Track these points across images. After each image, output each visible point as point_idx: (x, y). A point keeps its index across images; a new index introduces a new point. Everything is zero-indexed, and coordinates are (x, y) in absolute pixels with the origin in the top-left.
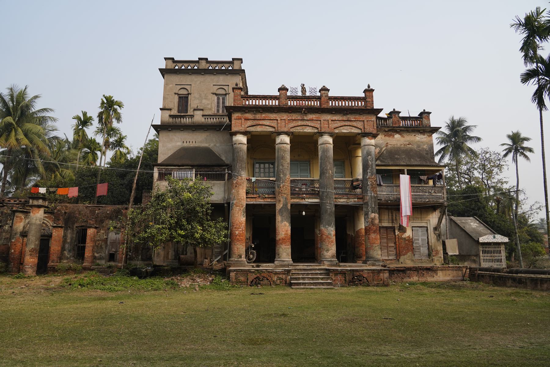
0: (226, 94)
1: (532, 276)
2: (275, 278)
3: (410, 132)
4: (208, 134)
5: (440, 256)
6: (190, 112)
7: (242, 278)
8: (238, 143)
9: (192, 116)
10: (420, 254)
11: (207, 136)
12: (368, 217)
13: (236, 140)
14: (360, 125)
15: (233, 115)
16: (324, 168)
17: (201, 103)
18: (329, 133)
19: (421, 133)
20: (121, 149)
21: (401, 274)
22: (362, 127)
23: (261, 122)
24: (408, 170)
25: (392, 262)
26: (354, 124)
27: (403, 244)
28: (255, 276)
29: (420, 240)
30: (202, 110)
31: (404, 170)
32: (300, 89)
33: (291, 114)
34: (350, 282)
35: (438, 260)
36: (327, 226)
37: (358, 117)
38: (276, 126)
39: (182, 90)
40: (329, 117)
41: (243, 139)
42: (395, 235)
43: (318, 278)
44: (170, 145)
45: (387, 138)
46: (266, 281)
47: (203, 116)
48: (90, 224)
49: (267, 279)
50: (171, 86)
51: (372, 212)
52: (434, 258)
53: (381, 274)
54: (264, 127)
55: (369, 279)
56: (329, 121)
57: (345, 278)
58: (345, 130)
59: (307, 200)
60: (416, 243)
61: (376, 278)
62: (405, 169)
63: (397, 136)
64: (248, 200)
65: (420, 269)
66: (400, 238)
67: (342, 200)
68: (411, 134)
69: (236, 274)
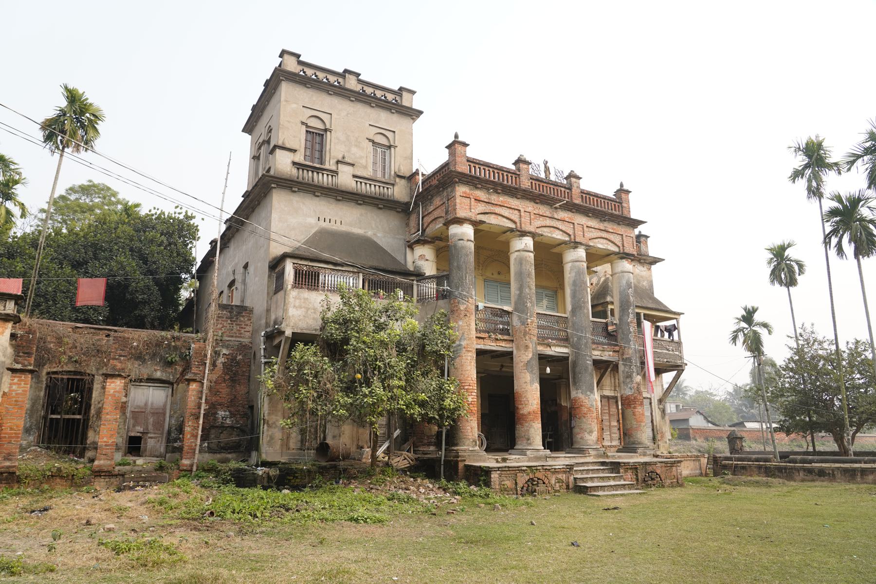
0: (390, 147)
1: (842, 465)
4: (363, 211)
6: (330, 165)
7: (508, 483)
8: (465, 239)
9: (335, 173)
11: (361, 215)
12: (632, 381)
13: (455, 235)
14: (617, 239)
15: (457, 188)
16: (579, 300)
17: (349, 151)
19: (640, 263)
20: (9, 205)
22: (620, 244)
23: (498, 210)
24: (645, 315)
30: (353, 165)
32: (542, 168)
33: (539, 206)
34: (644, 481)
36: (588, 393)
38: (517, 220)
39: (313, 119)
41: (468, 231)
44: (293, 221)
46: (541, 488)
47: (354, 176)
48: (114, 368)
50: (294, 106)
53: (674, 469)
54: (500, 218)
57: (637, 475)
59: (553, 348)
69: (500, 475)
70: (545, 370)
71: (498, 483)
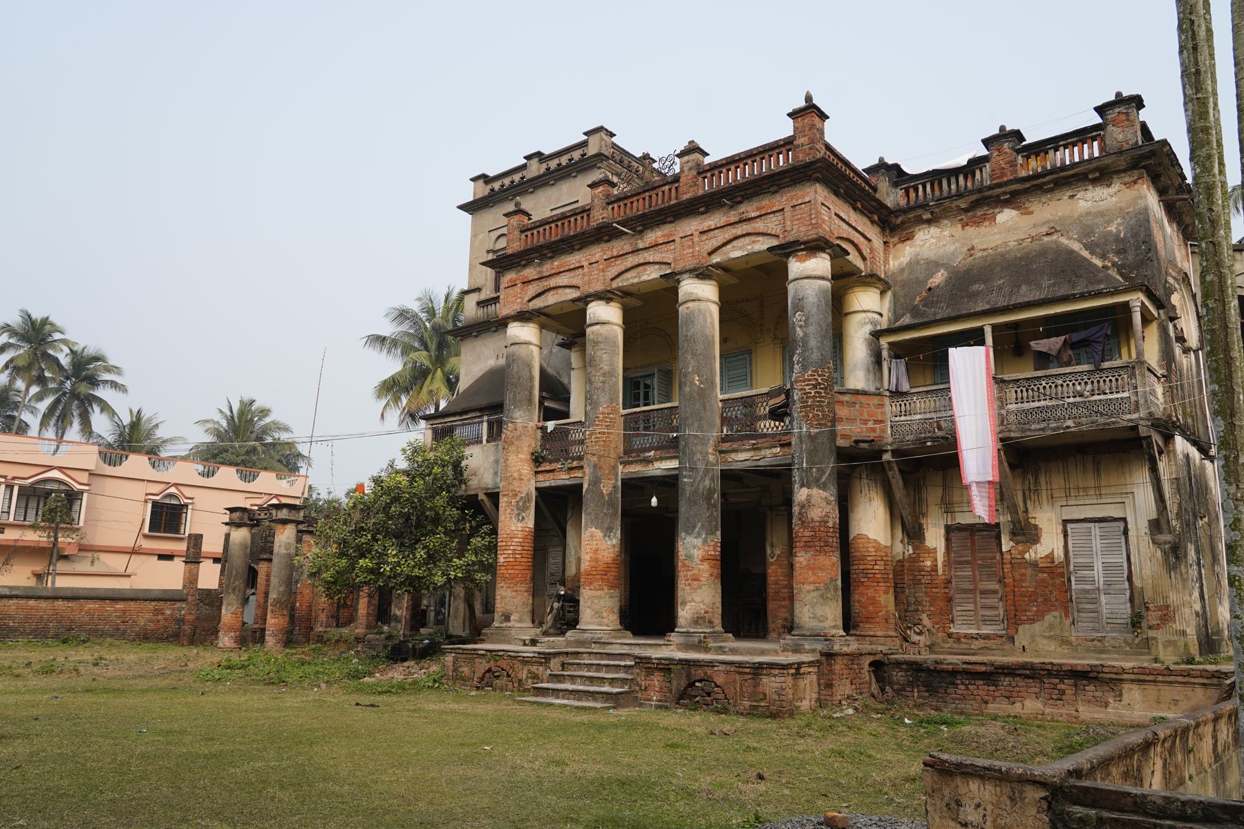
3: (1051, 190)
5: (1178, 626)
10: (1096, 620)
18: (690, 271)
19: (1095, 182)
23: (552, 282)
24: (995, 328)
25: (990, 643)
26: (759, 226)
27: (1028, 585)
28: (487, 666)
29: (1098, 566)
31: (980, 331)
35: (1169, 643)
37: (767, 203)
40: (692, 225)
42: (1002, 553)
43: (602, 680)
45: (970, 230)
49: (508, 676)
51: (802, 486)
52: (1151, 633)
54: (560, 291)
55: (731, 692)
56: (693, 239)
58: (735, 252)
59: (657, 465)
60: (1080, 580)
61: (750, 689)
62: (987, 324)
63: (1006, 216)
64: (540, 477)
65: (1050, 674)
67: (742, 456)
68: (1058, 194)
71: (451, 668)
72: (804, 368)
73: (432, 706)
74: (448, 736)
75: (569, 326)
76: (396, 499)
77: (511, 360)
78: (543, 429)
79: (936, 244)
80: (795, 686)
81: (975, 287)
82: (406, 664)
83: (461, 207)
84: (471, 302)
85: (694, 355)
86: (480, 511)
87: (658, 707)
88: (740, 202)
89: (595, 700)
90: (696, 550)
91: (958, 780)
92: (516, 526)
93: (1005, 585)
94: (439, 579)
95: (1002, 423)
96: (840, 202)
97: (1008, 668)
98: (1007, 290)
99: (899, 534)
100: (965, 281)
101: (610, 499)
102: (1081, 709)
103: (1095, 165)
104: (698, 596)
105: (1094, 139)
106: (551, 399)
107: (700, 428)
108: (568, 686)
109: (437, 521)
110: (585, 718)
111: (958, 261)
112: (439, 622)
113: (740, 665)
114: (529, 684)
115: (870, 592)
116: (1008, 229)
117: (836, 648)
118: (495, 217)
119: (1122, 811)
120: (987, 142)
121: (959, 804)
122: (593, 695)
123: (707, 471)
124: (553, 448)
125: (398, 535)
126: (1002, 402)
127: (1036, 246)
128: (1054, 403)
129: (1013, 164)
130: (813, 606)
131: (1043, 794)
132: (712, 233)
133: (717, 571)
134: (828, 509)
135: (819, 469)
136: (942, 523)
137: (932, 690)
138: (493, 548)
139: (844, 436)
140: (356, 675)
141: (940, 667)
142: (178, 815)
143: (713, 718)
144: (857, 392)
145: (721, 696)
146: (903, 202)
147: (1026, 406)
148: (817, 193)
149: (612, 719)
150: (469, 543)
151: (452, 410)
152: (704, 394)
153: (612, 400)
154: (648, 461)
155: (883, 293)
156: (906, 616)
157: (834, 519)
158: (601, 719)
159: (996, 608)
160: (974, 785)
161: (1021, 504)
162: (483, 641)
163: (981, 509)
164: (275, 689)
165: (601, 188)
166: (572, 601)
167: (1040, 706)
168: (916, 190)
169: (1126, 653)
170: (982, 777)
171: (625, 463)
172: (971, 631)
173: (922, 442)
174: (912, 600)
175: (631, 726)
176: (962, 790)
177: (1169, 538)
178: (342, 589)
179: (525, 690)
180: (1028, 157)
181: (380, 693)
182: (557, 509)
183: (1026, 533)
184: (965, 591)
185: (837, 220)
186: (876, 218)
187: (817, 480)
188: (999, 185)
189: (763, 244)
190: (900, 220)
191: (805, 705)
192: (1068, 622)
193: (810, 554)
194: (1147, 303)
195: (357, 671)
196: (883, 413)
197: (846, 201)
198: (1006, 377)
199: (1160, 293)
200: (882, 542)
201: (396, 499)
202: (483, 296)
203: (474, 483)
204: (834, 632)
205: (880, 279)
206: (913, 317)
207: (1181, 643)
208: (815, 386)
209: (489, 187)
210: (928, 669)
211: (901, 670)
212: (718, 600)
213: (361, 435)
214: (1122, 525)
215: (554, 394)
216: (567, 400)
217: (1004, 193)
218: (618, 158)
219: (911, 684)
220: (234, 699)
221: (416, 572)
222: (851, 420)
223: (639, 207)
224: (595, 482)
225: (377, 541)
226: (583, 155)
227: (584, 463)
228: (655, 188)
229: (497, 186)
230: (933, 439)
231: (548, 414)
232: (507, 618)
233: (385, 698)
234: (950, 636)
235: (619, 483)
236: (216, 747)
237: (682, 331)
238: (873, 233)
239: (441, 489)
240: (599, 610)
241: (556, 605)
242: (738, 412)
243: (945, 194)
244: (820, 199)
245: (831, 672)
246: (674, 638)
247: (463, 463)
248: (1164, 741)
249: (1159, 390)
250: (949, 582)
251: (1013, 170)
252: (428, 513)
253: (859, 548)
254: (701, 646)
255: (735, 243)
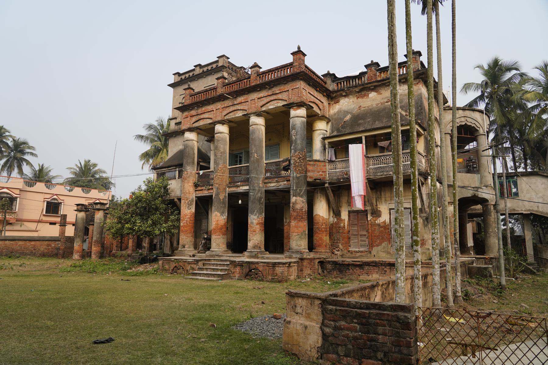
2: (189, 268)
5: (427, 247)
18: (254, 113)
21: (358, 271)
23: (202, 116)
24: (366, 137)
25: (363, 254)
26: (280, 96)
27: (377, 233)
31: (361, 138)
45: (360, 100)
51: (294, 196)
54: (205, 120)
55: (264, 273)
56: (255, 101)
58: (271, 106)
59: (241, 188)
61: (272, 272)
62: (363, 136)
63: (372, 95)
64: (197, 192)
65: (382, 265)
66: (374, 225)
67: (273, 185)
70: (242, 202)
72: (295, 151)
73: (151, 280)
74: (153, 291)
75: (208, 132)
76: (140, 201)
77: (186, 146)
78: (198, 174)
79: (347, 104)
80: (288, 271)
81: (360, 121)
82: (145, 265)
83: (169, 85)
84: (173, 123)
85: (255, 146)
86: (174, 205)
87: (238, 279)
88: (273, 87)
89: (214, 277)
90: (255, 220)
91: (296, 299)
92: (188, 211)
93: (369, 233)
94: (157, 232)
95: (367, 173)
96: (310, 88)
97: (368, 263)
98: (371, 123)
99: (332, 214)
100: (357, 118)
101: (223, 201)
102: (392, 277)
103: (403, 77)
104: (256, 238)
105: (404, 67)
106: (203, 162)
107: (257, 174)
108: (205, 272)
109: (157, 209)
110: (209, 284)
111: (355, 111)
112: (161, 249)
113: (268, 263)
114: (191, 271)
115: (320, 236)
116: (374, 99)
117: (305, 256)
118: (181, 90)
119: (343, 307)
120: (366, 66)
121: (296, 306)
122: (214, 275)
123: (259, 190)
124: (204, 180)
125: (141, 215)
126: (368, 165)
127: (382, 106)
128: (386, 165)
129: (375, 75)
130: (297, 241)
131: (320, 302)
132: (262, 99)
133: (263, 228)
134: (303, 205)
135: (300, 190)
136: (347, 210)
137: (341, 271)
138: (178, 220)
139: (311, 177)
140: (125, 269)
141: (344, 263)
142: (35, 319)
143: (257, 283)
144: (316, 161)
145: (261, 275)
146: (336, 88)
147: (376, 166)
148: (301, 84)
149: (220, 284)
150: (170, 218)
151: (165, 166)
152: (258, 161)
153: (224, 162)
154: (238, 186)
155: (328, 123)
156: (333, 245)
157: (305, 208)
158: (215, 284)
159: (365, 241)
160: (300, 300)
161: (375, 203)
162: (174, 256)
163: (359, 204)
164: (91, 275)
165: (221, 80)
166: (209, 240)
167: (378, 276)
168: (341, 84)
169: (409, 257)
170: (302, 297)
171: (229, 187)
172: (356, 249)
173: (339, 179)
174: (336, 238)
175: (225, 286)
176: (297, 302)
177: (425, 215)
178: (120, 235)
179: (189, 274)
180: (381, 73)
181: (132, 276)
182: (204, 205)
183: (376, 213)
184: (355, 235)
185: (309, 95)
186: (325, 94)
187: (299, 194)
188: (370, 83)
189: (281, 104)
190: (334, 95)
191: (292, 277)
192: (390, 246)
193: (296, 222)
194: (419, 129)
195: (125, 267)
196: (326, 169)
197: (313, 88)
198: (369, 156)
199: (425, 125)
200: (325, 217)
201: (140, 201)
202: (178, 121)
203: (173, 194)
204: (304, 250)
205: (326, 118)
206: (337, 132)
207: (428, 253)
208: (299, 158)
209: (180, 77)
210: (340, 264)
211: (330, 264)
212: (263, 239)
213: (127, 176)
214: (409, 210)
215: (204, 159)
216: (209, 162)
217: (372, 86)
218: (231, 67)
219: (333, 269)
220: (74, 278)
221: (148, 229)
222: (313, 171)
223: (235, 88)
224: (217, 194)
225: (133, 217)
226: (217, 66)
227: (214, 187)
228: (241, 81)
229: (183, 77)
230: (343, 179)
231: (202, 168)
232: (184, 247)
233: (134, 277)
234: (349, 251)
235: (227, 195)
236: (59, 296)
237: (251, 137)
238: (324, 100)
239: (159, 197)
240: (219, 244)
241: (203, 242)
242: (273, 168)
243: (351, 86)
244: (302, 87)
245: (302, 265)
246: (246, 253)
247: (168, 187)
248: (382, 285)
249: (423, 161)
250: (349, 232)
251: (373, 79)
252: (154, 205)
253: (316, 219)
254: (256, 257)
255: (271, 103)
